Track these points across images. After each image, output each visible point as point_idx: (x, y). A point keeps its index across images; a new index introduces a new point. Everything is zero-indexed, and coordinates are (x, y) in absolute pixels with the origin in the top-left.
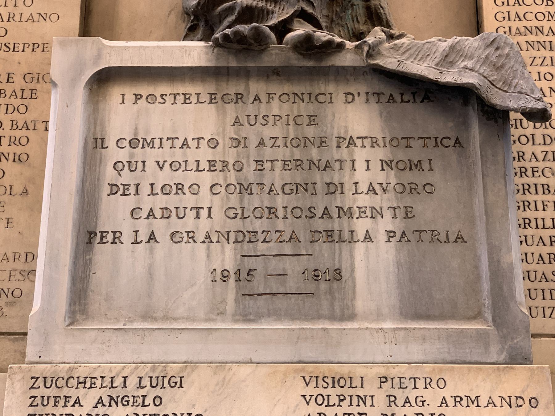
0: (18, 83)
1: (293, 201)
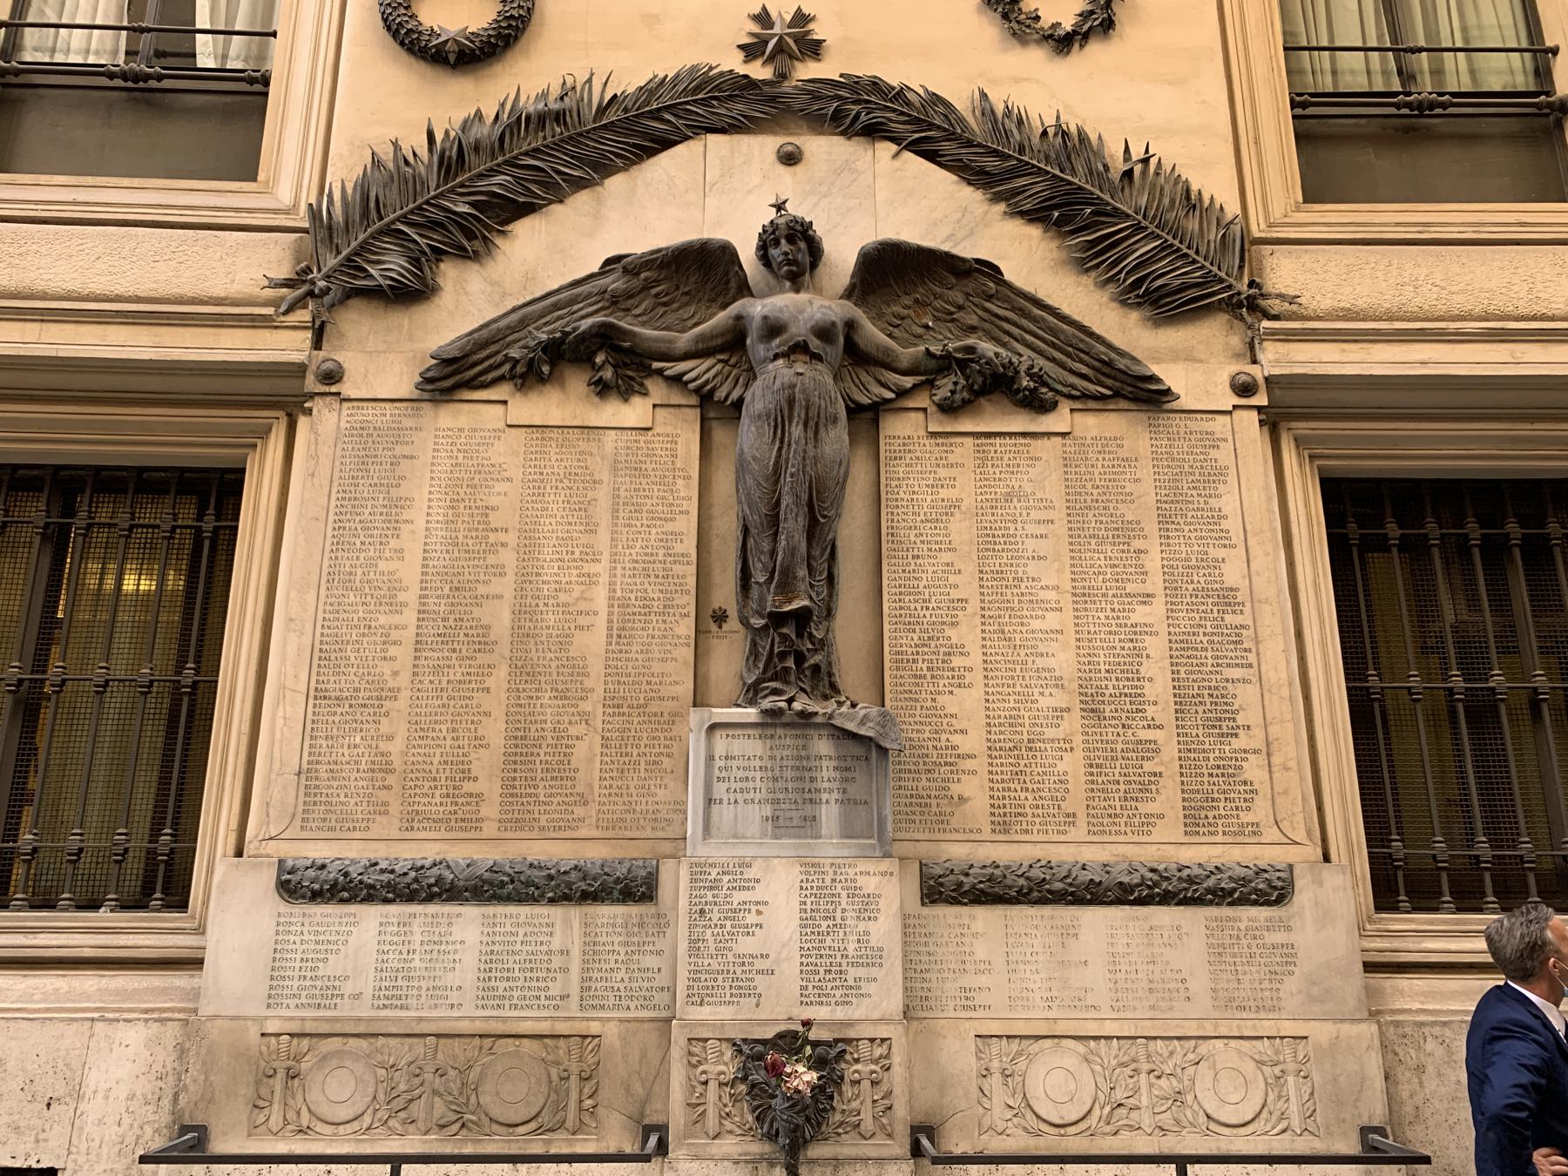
0: (666, 717)
1: (796, 785)
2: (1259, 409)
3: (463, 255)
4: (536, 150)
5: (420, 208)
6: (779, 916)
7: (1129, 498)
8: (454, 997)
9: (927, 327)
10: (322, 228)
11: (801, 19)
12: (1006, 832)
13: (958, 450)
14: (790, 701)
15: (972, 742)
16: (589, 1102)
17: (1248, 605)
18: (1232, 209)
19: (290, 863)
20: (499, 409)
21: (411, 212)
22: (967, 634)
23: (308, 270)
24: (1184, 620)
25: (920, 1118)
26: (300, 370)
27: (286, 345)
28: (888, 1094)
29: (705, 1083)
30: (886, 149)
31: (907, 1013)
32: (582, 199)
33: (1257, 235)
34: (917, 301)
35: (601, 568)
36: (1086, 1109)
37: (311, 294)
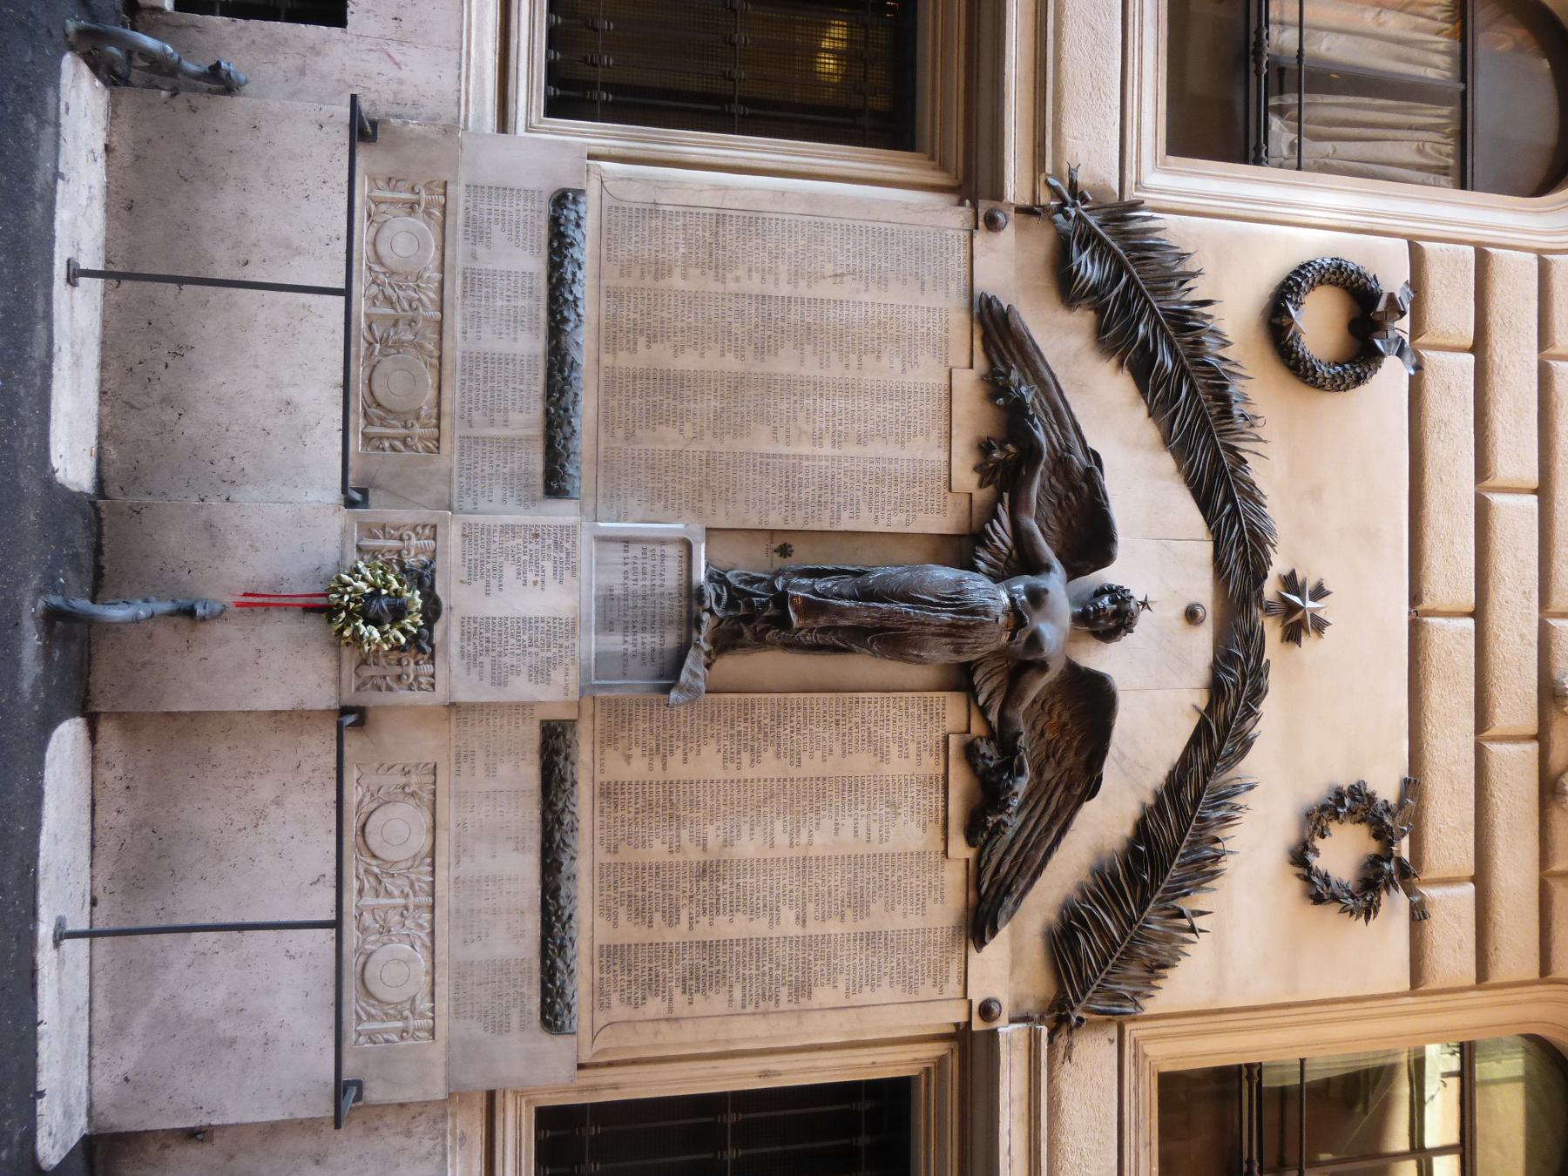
2: (969, 1023)
3: (1100, 331)
4: (1196, 392)
5: (1142, 294)
6: (538, 594)
7: (889, 907)
8: (471, 334)
9: (1042, 734)
10: (1120, 213)
11: (1320, 625)
12: (602, 794)
13: (932, 761)
14: (711, 611)
15: (677, 768)
16: (387, 444)
17: (796, 1007)
18: (1151, 1007)
19: (582, 199)
20: (965, 361)
21: (1138, 287)
22: (770, 766)
23: (1084, 200)
24: (779, 952)
25: (370, 716)
26: (997, 194)
27: (1016, 186)
28: (390, 689)
29: (401, 539)
30: (1202, 700)
31: (453, 706)
32: (1150, 432)
33: (1128, 1027)
34: (1066, 725)
35: (827, 449)
36: (377, 853)
37: (1065, 203)
